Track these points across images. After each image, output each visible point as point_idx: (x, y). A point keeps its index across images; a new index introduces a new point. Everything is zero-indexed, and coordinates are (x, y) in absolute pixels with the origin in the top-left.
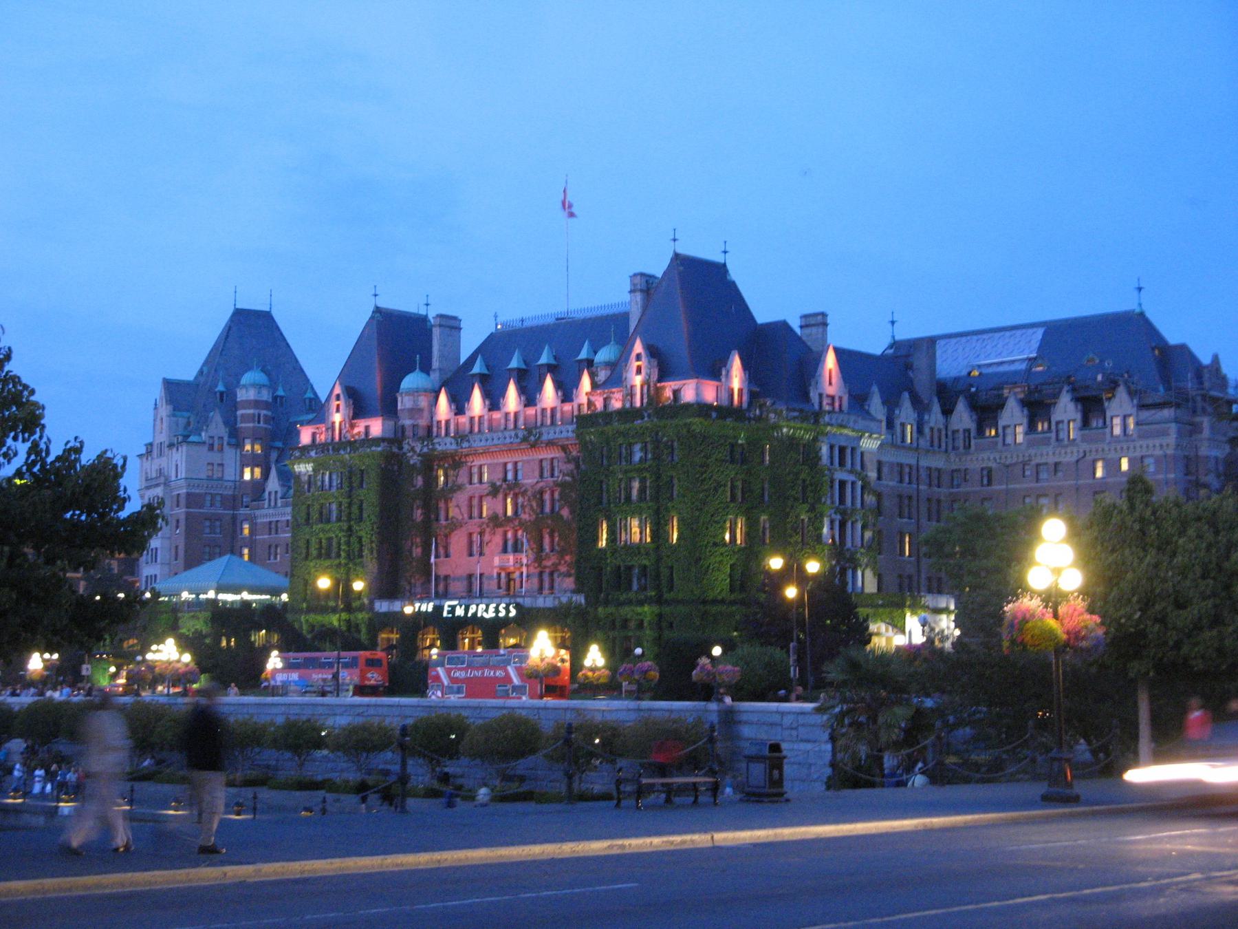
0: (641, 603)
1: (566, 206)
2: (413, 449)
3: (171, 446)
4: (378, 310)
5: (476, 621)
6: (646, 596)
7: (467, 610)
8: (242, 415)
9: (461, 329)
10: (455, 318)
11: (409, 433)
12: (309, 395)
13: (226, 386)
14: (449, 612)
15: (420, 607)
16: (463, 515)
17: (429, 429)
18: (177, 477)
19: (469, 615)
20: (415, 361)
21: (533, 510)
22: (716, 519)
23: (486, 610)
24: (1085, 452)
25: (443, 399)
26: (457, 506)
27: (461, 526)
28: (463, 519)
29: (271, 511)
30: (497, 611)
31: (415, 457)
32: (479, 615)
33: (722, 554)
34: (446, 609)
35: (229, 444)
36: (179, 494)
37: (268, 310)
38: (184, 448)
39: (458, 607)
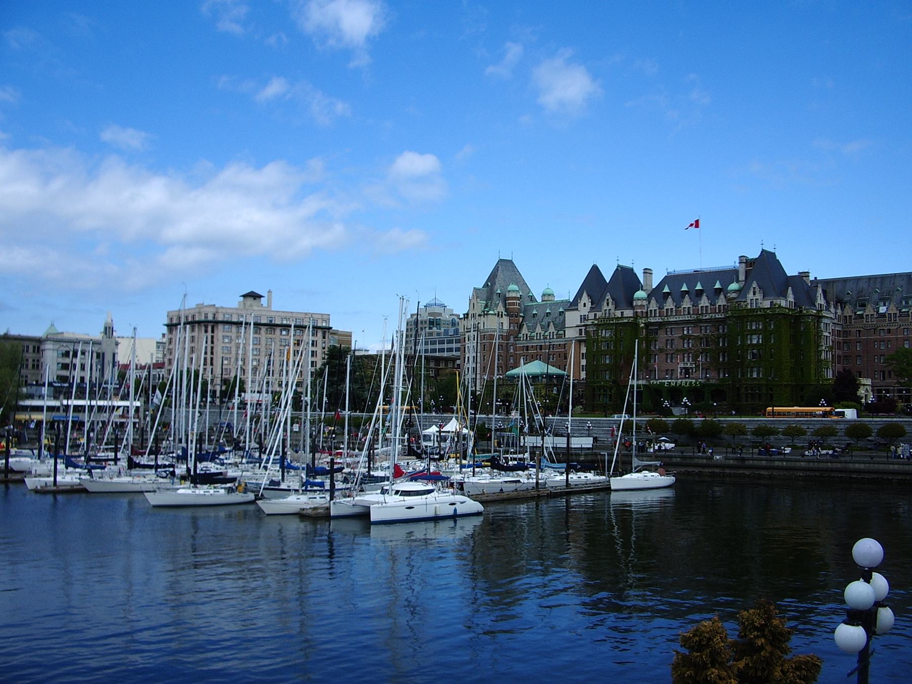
3: (480, 315)
4: (619, 266)
8: (508, 303)
10: (650, 270)
12: (531, 295)
13: (500, 291)
17: (647, 312)
29: (524, 342)
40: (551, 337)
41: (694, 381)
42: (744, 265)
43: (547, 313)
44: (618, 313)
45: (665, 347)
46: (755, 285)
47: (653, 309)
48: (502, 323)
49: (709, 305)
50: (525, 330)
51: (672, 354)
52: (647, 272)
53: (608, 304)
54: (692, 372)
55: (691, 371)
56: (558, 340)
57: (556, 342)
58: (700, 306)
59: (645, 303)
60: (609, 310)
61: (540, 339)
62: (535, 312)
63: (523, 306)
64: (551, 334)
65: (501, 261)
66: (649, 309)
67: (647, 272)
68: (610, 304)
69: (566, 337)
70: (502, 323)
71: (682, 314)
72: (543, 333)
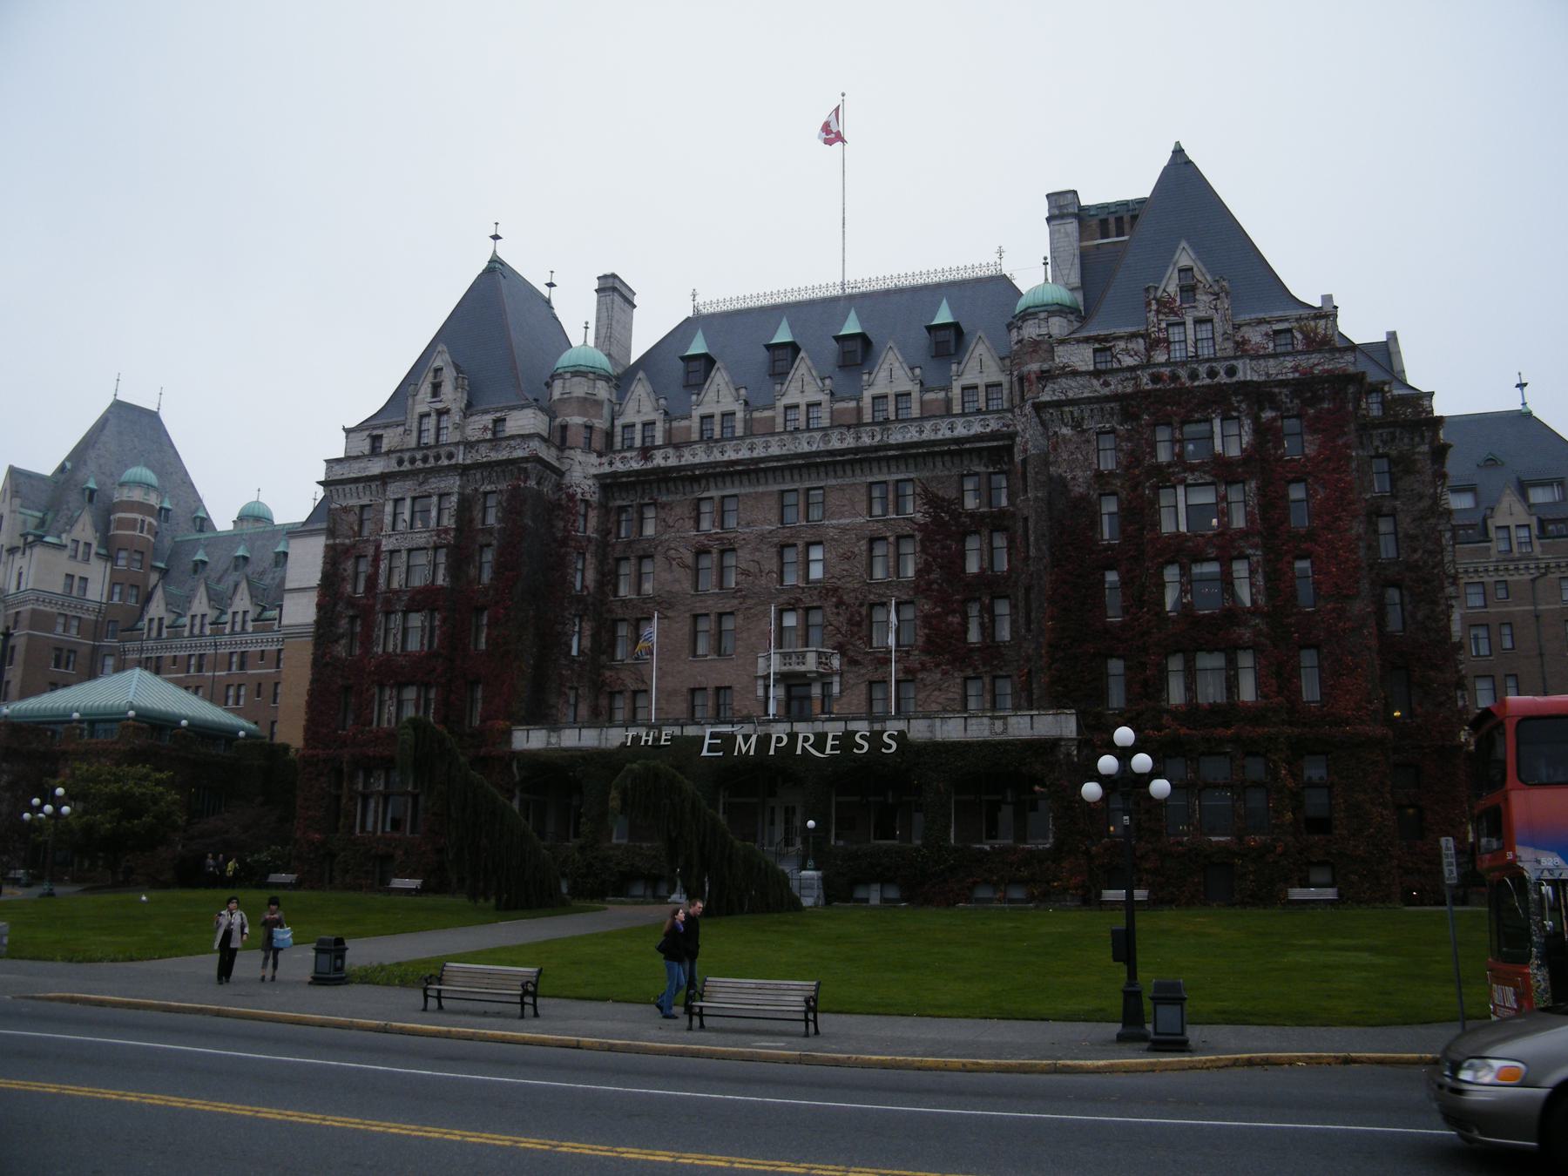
1: (831, 135)
8: (120, 520)
9: (635, 306)
11: (576, 437)
12: (201, 514)
13: (97, 483)
17: (609, 435)
18: (18, 588)
24: (1547, 567)
32: (799, 752)
34: (707, 741)
35: (97, 554)
36: (18, 613)
37: (156, 410)
38: (38, 551)
40: (238, 628)
41: (862, 727)
42: (1072, 226)
43: (237, 558)
44: (478, 425)
45: (687, 586)
46: (1185, 258)
47: (638, 420)
48: (84, 580)
49: (915, 389)
50: (157, 609)
51: (720, 615)
52: (613, 291)
53: (436, 388)
54: (826, 696)
55: (816, 691)
56: (260, 636)
57: (255, 643)
58: (867, 395)
59: (603, 391)
60: (441, 413)
61: (202, 634)
62: (200, 556)
63: (167, 542)
64: (239, 618)
65: (120, 409)
66: (619, 423)
67: (613, 291)
68: (447, 389)
69: (285, 622)
70: (84, 580)
71: (779, 429)
72: (212, 615)
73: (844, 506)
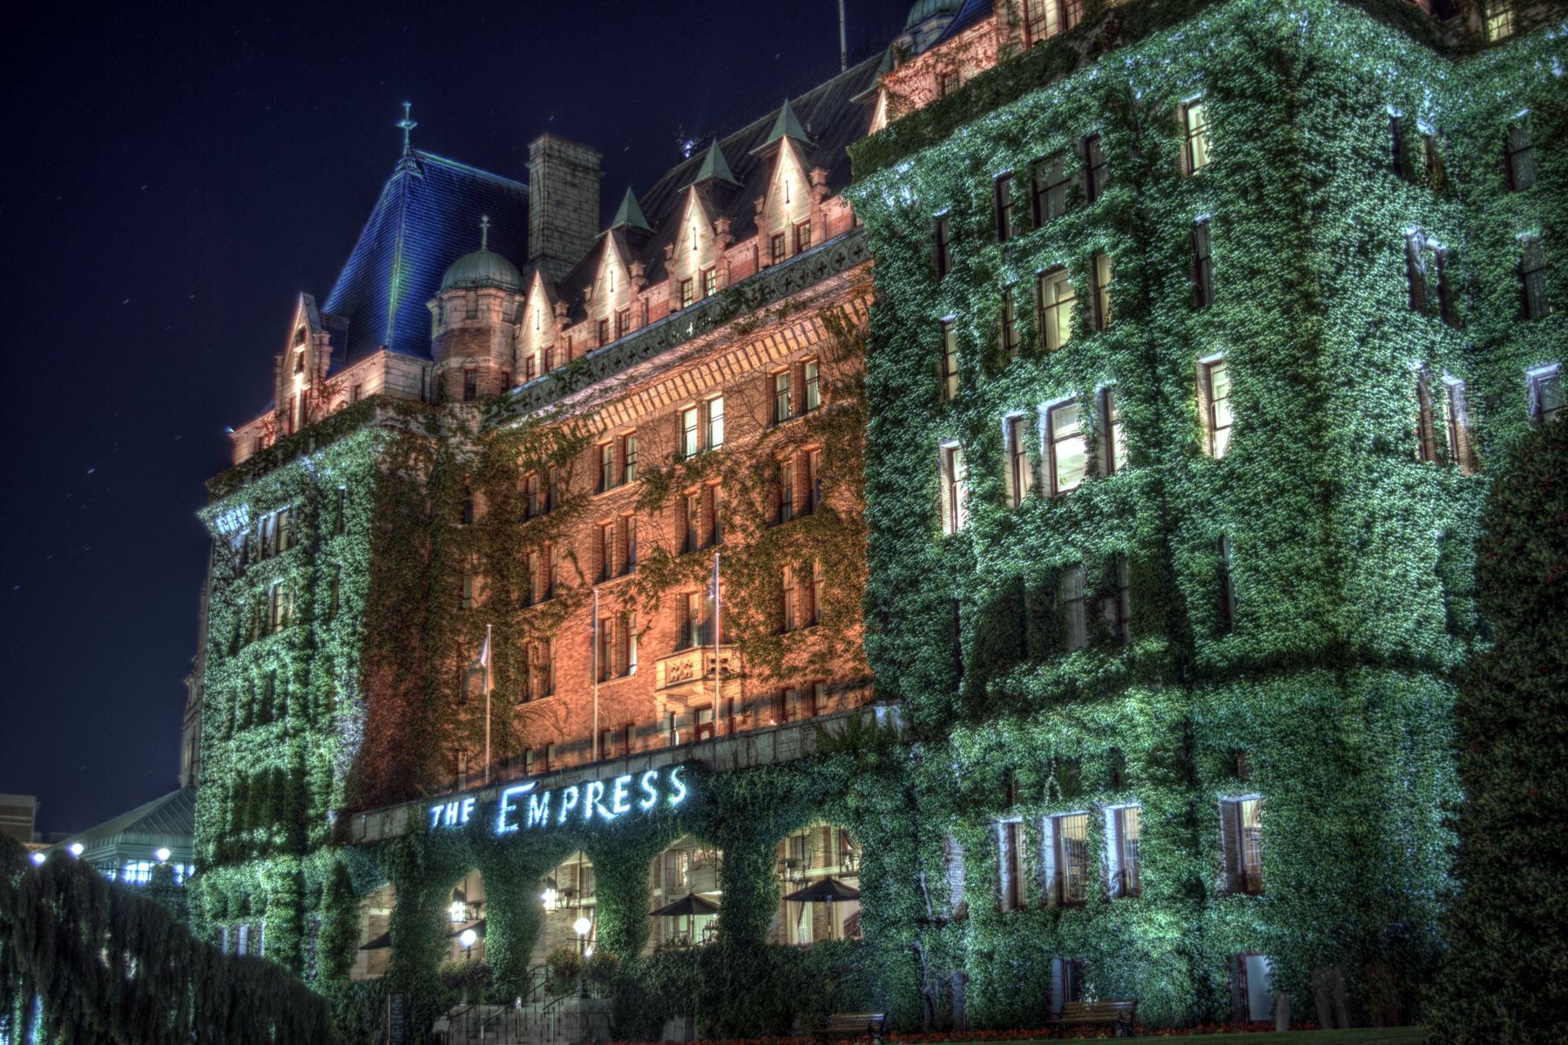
0: (1109, 689)
2: (463, 429)
5: (579, 831)
6: (1131, 662)
7: (555, 805)
14: (512, 818)
15: (443, 813)
16: (581, 574)
19: (562, 819)
20: (480, 231)
21: (755, 515)
22: (1378, 356)
23: (606, 800)
25: (537, 302)
26: (572, 555)
27: (578, 605)
28: (582, 585)
30: (635, 793)
31: (469, 447)
32: (588, 813)
33: (1408, 487)
39: (533, 800)
73: (743, 416)
